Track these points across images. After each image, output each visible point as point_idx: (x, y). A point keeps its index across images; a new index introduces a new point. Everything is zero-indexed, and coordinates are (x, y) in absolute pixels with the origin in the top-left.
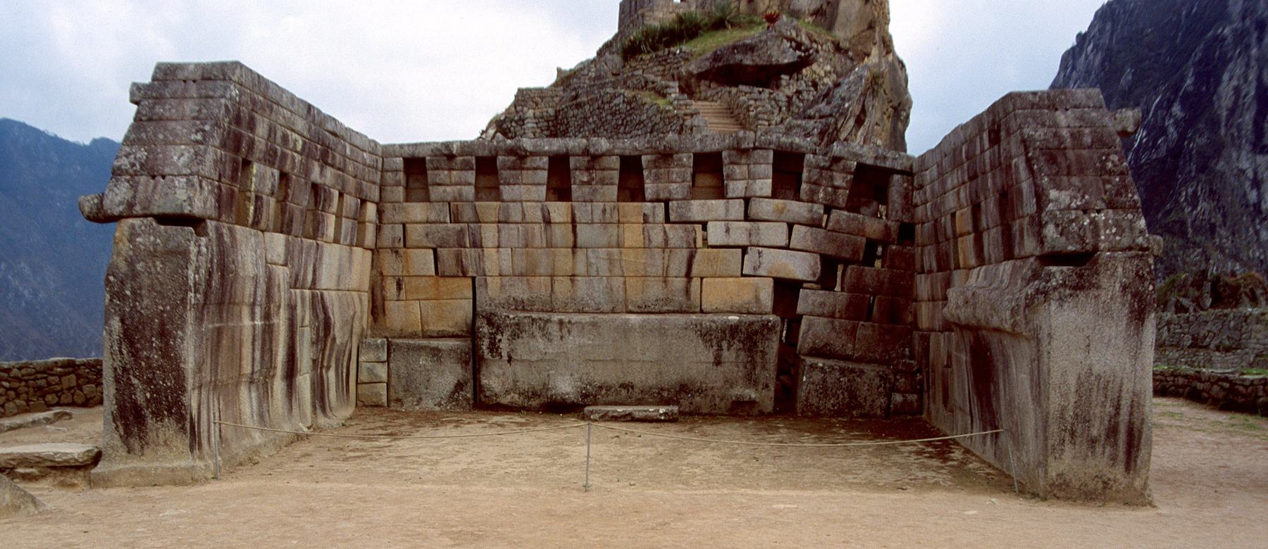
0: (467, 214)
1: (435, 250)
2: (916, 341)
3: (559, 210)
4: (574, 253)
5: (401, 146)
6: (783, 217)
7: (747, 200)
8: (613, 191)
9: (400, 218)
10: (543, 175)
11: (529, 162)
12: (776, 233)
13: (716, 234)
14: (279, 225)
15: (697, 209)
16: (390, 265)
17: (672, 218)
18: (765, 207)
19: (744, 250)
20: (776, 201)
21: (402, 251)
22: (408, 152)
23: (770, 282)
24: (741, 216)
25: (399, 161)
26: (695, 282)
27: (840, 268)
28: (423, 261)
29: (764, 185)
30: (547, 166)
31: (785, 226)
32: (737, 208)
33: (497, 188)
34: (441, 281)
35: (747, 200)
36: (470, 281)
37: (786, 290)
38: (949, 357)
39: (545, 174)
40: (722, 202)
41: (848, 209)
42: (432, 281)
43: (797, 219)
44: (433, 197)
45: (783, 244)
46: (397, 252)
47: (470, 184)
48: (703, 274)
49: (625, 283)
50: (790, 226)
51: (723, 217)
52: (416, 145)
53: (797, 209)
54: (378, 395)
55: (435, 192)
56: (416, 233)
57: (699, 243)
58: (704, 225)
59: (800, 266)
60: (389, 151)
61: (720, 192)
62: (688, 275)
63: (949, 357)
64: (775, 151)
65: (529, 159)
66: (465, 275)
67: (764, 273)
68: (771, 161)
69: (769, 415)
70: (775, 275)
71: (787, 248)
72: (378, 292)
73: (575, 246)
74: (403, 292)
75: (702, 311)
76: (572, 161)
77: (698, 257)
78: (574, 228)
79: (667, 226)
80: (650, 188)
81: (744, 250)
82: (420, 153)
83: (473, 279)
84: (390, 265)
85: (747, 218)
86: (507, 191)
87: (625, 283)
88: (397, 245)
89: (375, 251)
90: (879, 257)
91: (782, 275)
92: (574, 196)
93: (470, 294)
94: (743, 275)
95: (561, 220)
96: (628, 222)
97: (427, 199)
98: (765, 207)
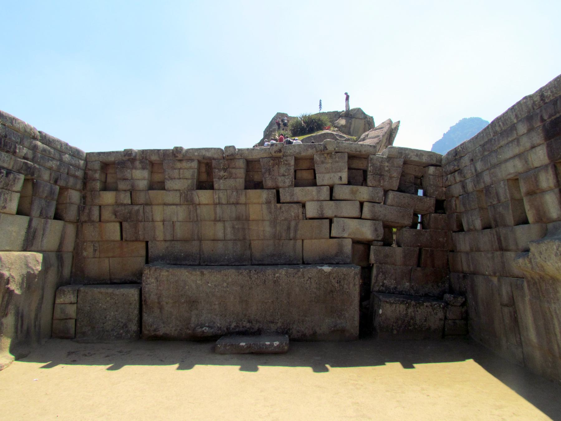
4: (215, 224)
12: (351, 209)
13: (311, 210)
15: (300, 193)
20: (351, 186)
23: (350, 240)
24: (328, 198)
25: (97, 166)
26: (299, 243)
32: (325, 192)
36: (144, 244)
50: (362, 204)
51: (316, 198)
57: (301, 216)
67: (346, 235)
70: (353, 236)
71: (360, 218)
74: (97, 253)
79: (279, 205)
85: (331, 199)
89: (79, 223)
91: (359, 237)
94: (331, 237)
95: (207, 202)
98: (342, 192)
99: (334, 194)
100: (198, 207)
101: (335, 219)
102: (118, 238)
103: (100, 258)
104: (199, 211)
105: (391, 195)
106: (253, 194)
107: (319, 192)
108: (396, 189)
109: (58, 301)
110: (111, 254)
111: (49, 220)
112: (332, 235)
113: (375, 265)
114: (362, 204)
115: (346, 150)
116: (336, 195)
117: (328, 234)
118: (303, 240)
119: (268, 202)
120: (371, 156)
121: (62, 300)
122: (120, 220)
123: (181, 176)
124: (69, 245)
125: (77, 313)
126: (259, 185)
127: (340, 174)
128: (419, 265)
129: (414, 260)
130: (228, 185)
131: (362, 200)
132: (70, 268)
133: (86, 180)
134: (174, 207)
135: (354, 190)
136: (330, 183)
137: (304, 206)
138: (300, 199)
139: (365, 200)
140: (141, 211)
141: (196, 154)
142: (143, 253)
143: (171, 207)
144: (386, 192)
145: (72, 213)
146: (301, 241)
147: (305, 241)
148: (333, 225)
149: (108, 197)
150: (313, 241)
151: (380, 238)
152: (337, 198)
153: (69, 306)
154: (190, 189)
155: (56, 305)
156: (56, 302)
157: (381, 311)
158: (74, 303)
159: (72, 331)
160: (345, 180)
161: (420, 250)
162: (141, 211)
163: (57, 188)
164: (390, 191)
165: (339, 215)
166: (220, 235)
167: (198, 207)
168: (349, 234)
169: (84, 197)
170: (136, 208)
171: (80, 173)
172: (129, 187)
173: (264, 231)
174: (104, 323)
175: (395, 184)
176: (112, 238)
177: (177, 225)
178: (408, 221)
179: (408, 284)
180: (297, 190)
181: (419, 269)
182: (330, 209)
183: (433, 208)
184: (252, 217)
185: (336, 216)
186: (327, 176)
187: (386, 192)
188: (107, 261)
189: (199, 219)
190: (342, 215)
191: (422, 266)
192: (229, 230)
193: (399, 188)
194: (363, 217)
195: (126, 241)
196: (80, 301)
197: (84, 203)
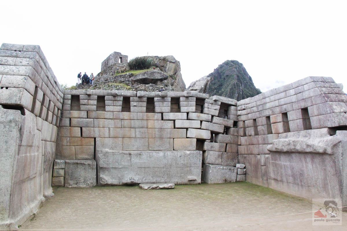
1: (81, 128)
3: (126, 115)
7: (188, 113)
9: (68, 116)
10: (121, 103)
12: (197, 124)
14: (102, 109)
19: (187, 129)
23: (195, 140)
25: (69, 97)
29: (193, 108)
31: (199, 122)
33: (105, 107)
34: (83, 139)
35: (188, 113)
36: (93, 139)
37: (200, 142)
41: (218, 116)
42: (79, 139)
43: (204, 119)
44: (82, 109)
45: (199, 127)
47: (95, 105)
48: (174, 137)
49: (148, 140)
50: (201, 122)
53: (203, 116)
54: (60, 182)
55: (82, 107)
57: (173, 127)
58: (174, 121)
61: (179, 110)
65: (117, 97)
68: (195, 100)
69: (199, 184)
70: (197, 137)
80: (157, 109)
81: (187, 129)
83: (95, 138)
85: (188, 119)
86: (107, 108)
87: (148, 140)
91: (199, 137)
93: (93, 144)
94: (187, 138)
95: (127, 118)
97: (79, 110)
98: (193, 115)
99: (189, 117)
100: (122, 120)
101: (189, 129)
102: (80, 136)
103: (70, 146)
104: (123, 123)
105: (215, 118)
108: (217, 115)
109: (55, 167)
110: (76, 144)
112: (187, 137)
113: (206, 151)
114: (201, 122)
115: (196, 96)
116: (190, 117)
118: (174, 139)
121: (57, 167)
123: (114, 105)
125: (65, 174)
128: (226, 151)
129: (223, 150)
131: (201, 120)
134: (110, 120)
135: (198, 115)
136: (187, 111)
139: (202, 120)
143: (109, 120)
147: (175, 139)
148: (188, 131)
149: (75, 113)
151: (209, 138)
152: (190, 119)
153: (61, 170)
155: (54, 170)
157: (210, 172)
158: (63, 169)
160: (194, 110)
164: (214, 117)
165: (191, 127)
166: (133, 135)
168: (196, 136)
173: (155, 133)
174: (79, 179)
175: (216, 113)
176: (77, 136)
177: (111, 129)
178: (222, 131)
179: (220, 160)
181: (225, 153)
182: (187, 124)
184: (149, 127)
186: (186, 108)
187: (213, 116)
188: (74, 147)
189: (122, 127)
191: (227, 152)
194: (202, 128)
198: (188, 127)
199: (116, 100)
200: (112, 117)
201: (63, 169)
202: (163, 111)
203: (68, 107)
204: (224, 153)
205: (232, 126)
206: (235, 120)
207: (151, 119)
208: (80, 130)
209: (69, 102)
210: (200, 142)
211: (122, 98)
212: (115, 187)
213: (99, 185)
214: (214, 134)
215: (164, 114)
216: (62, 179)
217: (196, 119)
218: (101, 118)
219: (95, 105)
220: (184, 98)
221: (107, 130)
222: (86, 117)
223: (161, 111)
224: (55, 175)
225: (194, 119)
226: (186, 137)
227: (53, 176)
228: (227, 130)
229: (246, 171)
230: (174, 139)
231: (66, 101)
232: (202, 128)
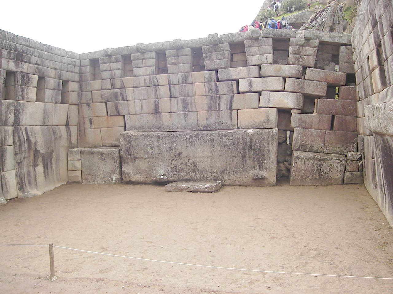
0: (118, 83)
1: (106, 103)
2: (359, 141)
3: (162, 78)
4: (170, 100)
5: (88, 54)
6: (279, 74)
7: (260, 66)
8: (188, 67)
9: (89, 88)
11: (146, 56)
12: (276, 84)
13: (243, 86)
16: (86, 111)
17: (220, 78)
18: (268, 69)
21: (91, 105)
22: (91, 57)
24: (257, 75)
25: (87, 62)
26: (234, 112)
27: (316, 100)
28: (101, 108)
30: (154, 57)
32: (254, 71)
34: (109, 118)
35: (260, 66)
36: (122, 117)
38: (373, 153)
39: (154, 60)
40: (245, 68)
41: (315, 66)
42: (105, 118)
43: (287, 74)
45: (280, 88)
46: (89, 106)
47: (119, 69)
50: (285, 79)
51: (246, 76)
52: (94, 53)
53: (286, 69)
56: (97, 94)
57: (235, 91)
59: (289, 101)
60: (81, 57)
62: (231, 109)
63: (373, 153)
64: (273, 39)
65: (146, 54)
66: (119, 115)
71: (283, 91)
72: (82, 125)
73: (171, 97)
74: (92, 125)
75: (238, 128)
76: (167, 52)
77: (235, 99)
78: (170, 87)
79: (217, 83)
80: (208, 64)
81: (260, 93)
82: (96, 56)
83: (124, 116)
84: (86, 111)
85: (260, 76)
86: (137, 71)
88: (89, 101)
89: (79, 105)
90: (337, 94)
92: (169, 71)
93: (123, 124)
95: (164, 83)
96: (197, 82)
98: (268, 69)
101: (262, 93)
102: (105, 114)
105: (308, 71)
106: (197, 74)
107: (249, 71)
108: (312, 65)
111: (58, 104)
114: (285, 79)
115: (271, 35)
117: (257, 104)
119: (210, 81)
120: (291, 40)
122: (105, 101)
124: (74, 120)
126: (202, 68)
127: (265, 56)
128: (332, 128)
130: (179, 68)
131: (284, 76)
132: (76, 137)
133: (81, 73)
136: (259, 63)
137: (237, 81)
138: (234, 77)
139: (286, 76)
140: (119, 93)
141: (154, 47)
142: (122, 124)
144: (304, 68)
145: (73, 97)
146: (236, 111)
147: (239, 111)
149: (96, 84)
150: (246, 110)
151: (300, 108)
154: (153, 74)
156: (69, 159)
159: (80, 179)
160: (270, 60)
161: (333, 117)
162: (119, 93)
163: (62, 81)
165: (265, 89)
166: (175, 109)
167: (157, 88)
169: (81, 86)
170: (115, 91)
171: (77, 69)
172: (109, 77)
175: (311, 61)
177: (144, 101)
180: (232, 69)
182: (258, 84)
183: (345, 81)
184: (197, 93)
185: (263, 91)
187: (304, 68)
190: (268, 89)
192: (180, 104)
193: (316, 64)
194: (285, 90)
195: (111, 116)
196: (82, 159)
197: (81, 91)
198: (261, 90)
199: (144, 59)
200: (142, 84)
201: (80, 160)
202: (216, 67)
203: (88, 76)
204: (329, 131)
205: (343, 82)
206: (350, 72)
207: (199, 81)
208: (105, 107)
209: (88, 69)
210: (284, 113)
211: (153, 54)
212: (138, 186)
213: (125, 181)
214: (308, 101)
215: (218, 71)
216: (78, 173)
217: (273, 75)
218: (129, 87)
219: (119, 69)
220: (250, 41)
221: (138, 102)
222: (110, 87)
223: (213, 68)
224: (70, 168)
225: (270, 75)
226: (257, 106)
227: (68, 170)
228: (331, 90)
229: (362, 165)
230: (237, 110)
231: (83, 69)
232: (285, 90)
